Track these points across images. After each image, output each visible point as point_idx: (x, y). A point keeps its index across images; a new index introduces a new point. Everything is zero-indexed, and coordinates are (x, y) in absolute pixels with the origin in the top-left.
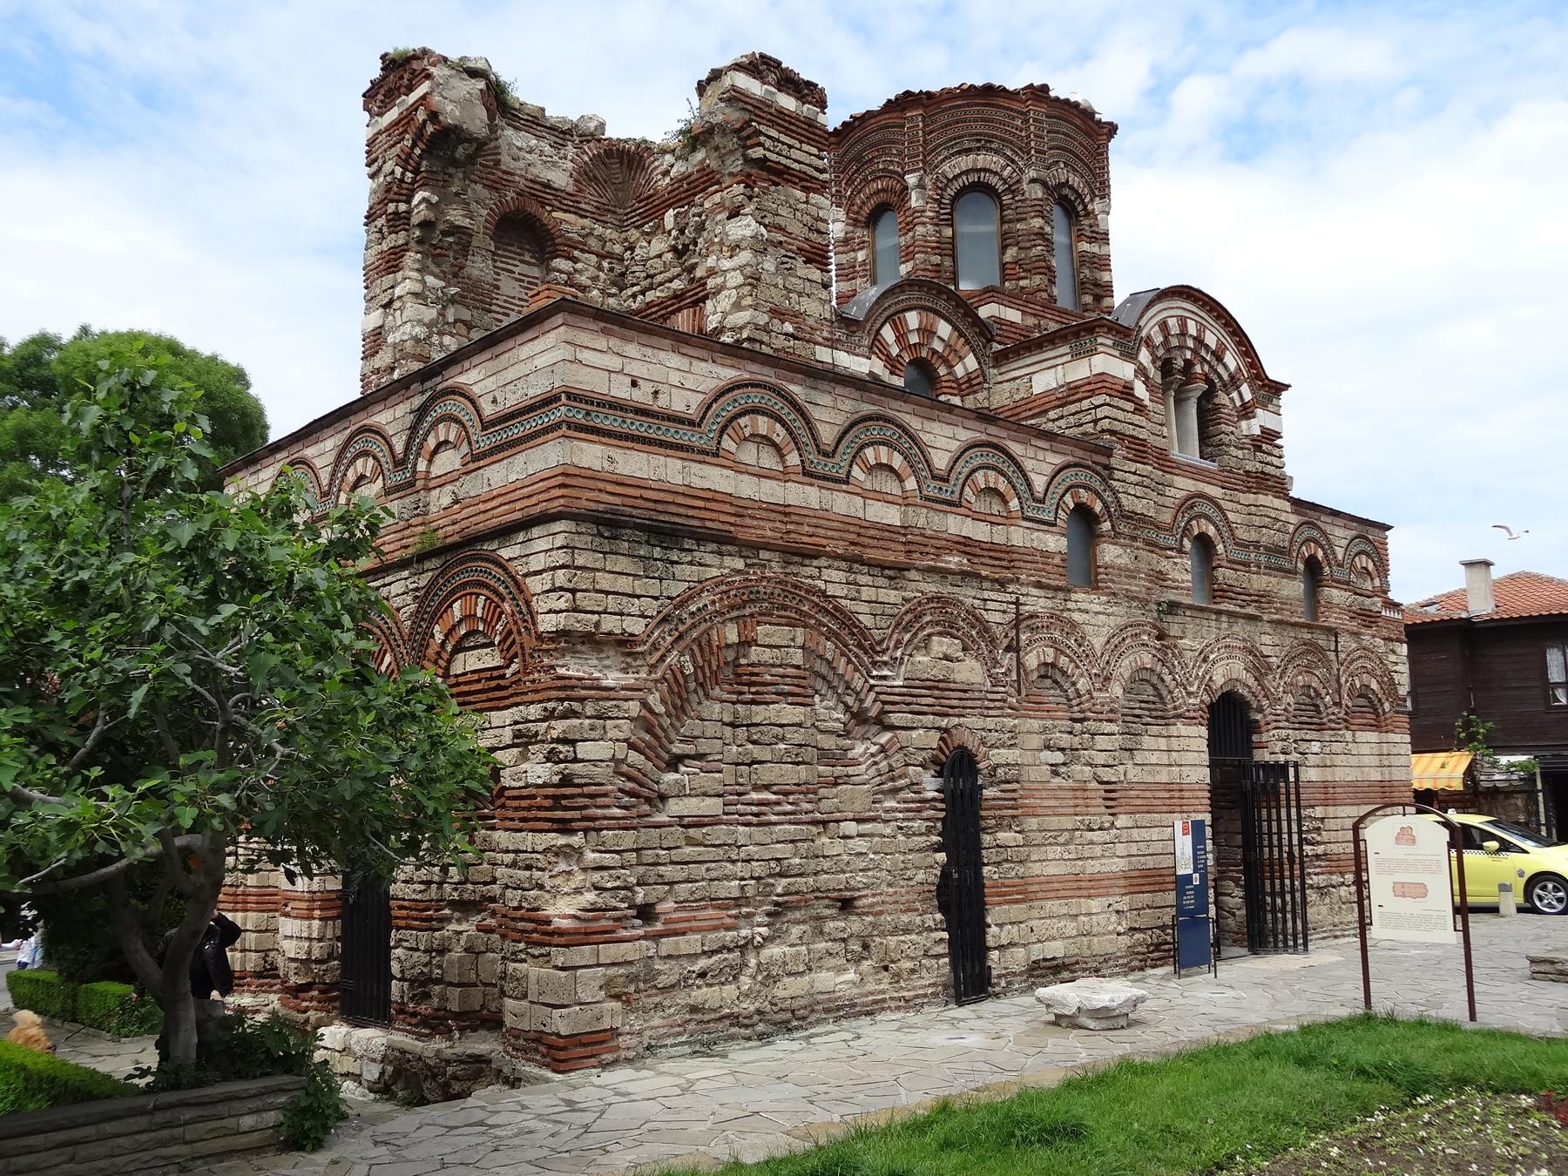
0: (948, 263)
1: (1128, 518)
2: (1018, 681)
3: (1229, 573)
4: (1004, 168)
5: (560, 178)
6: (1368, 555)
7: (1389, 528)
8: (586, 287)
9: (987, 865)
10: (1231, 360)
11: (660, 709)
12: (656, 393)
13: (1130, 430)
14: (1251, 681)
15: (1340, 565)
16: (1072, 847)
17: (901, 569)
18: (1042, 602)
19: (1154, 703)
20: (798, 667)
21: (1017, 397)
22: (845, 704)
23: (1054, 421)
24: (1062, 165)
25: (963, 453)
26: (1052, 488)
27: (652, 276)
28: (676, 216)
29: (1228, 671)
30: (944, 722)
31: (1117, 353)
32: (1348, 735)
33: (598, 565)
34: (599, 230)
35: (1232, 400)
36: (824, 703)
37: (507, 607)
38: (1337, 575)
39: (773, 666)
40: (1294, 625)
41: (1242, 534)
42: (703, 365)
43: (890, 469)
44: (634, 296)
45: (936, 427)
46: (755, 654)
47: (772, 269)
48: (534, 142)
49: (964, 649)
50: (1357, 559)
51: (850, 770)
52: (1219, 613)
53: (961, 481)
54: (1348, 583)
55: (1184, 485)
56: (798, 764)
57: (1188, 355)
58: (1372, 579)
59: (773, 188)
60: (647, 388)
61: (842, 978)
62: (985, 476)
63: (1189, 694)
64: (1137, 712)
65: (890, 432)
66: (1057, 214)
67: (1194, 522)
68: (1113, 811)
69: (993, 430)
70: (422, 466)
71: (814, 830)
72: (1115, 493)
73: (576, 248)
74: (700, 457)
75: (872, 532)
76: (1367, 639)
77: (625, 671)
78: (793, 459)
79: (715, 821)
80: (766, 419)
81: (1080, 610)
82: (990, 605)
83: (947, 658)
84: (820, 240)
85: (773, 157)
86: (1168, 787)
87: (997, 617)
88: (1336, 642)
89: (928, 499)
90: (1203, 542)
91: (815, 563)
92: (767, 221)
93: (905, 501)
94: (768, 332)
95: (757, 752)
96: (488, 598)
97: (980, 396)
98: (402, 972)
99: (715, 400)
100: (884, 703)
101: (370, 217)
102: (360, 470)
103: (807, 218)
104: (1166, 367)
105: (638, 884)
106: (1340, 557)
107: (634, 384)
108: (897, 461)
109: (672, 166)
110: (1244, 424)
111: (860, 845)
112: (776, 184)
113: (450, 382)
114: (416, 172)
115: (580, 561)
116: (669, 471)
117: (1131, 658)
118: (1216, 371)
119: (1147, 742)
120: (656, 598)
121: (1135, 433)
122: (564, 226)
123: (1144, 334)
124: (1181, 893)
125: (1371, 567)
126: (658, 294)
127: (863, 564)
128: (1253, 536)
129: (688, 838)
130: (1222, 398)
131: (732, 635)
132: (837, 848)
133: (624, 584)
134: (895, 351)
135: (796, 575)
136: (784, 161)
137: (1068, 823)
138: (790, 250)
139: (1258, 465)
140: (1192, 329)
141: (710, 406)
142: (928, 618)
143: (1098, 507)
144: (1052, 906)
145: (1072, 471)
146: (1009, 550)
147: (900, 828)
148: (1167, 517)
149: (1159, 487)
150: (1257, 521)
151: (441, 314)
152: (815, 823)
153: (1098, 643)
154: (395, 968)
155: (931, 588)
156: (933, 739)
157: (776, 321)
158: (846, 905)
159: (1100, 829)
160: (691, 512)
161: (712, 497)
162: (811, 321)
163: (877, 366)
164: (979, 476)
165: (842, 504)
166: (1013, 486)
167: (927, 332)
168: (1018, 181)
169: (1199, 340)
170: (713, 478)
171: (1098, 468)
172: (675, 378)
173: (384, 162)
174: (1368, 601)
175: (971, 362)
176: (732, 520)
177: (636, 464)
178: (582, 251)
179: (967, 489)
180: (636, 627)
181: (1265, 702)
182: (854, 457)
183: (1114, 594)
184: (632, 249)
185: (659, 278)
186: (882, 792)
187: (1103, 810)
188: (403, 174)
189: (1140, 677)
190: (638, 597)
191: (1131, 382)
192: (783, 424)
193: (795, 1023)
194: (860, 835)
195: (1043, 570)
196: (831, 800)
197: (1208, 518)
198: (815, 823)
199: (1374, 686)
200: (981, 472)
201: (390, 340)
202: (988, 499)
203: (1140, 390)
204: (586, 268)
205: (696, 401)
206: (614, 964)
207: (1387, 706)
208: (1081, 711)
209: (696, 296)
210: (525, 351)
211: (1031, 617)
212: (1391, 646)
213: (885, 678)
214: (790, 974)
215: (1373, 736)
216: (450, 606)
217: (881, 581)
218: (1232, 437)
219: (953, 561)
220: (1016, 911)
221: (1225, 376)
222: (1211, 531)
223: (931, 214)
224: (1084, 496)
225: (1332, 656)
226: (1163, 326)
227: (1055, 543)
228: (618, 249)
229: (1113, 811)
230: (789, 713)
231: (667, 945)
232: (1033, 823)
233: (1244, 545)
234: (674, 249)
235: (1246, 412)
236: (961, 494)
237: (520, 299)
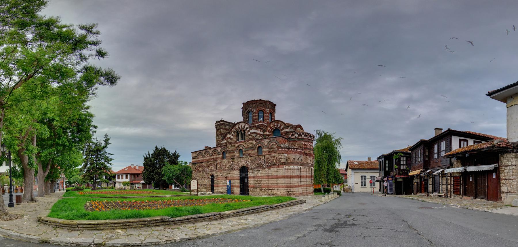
13: (230, 142)
17: (208, 162)
29: (242, 163)
32: (266, 169)
38: (264, 147)
40: (254, 156)
46: (200, 170)
55: (237, 144)
57: (240, 129)
76: (273, 155)
86: (234, 177)
95: (200, 176)
104: (237, 132)
111: (207, 182)
119: (231, 172)
124: (227, 187)
125: (275, 143)
137: (222, 180)
146: (217, 158)
148: (235, 149)
149: (234, 146)
161: (198, 161)
165: (205, 158)
169: (241, 127)
170: (198, 159)
181: (248, 167)
189: (230, 166)
199: (275, 161)
209: (26, 190)
212: (280, 155)
215: (275, 169)
219: (212, 160)
220: (217, 187)
225: (264, 159)
227: (221, 156)
233: (247, 148)
235: (249, 131)
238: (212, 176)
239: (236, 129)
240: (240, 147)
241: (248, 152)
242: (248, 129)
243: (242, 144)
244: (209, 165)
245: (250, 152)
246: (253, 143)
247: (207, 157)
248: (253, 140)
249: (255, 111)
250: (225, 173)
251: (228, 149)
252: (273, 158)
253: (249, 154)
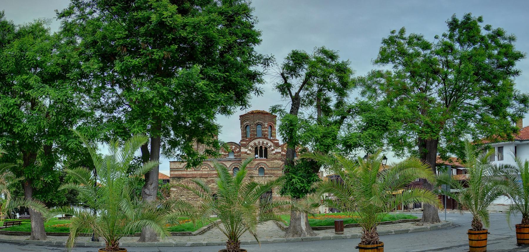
0: (245, 135)
10: (269, 145)
41: (270, 166)
55: (257, 162)
65: (205, 165)
78: (193, 169)
116: (180, 173)
130: (268, 149)
140: (261, 142)
148: (254, 166)
155: (211, 179)
161: (183, 174)
165: (199, 172)
169: (263, 143)
170: (185, 173)
177: (176, 173)
196: (198, 199)
219: (214, 176)
222: (263, 166)
224: (236, 166)
235: (273, 150)
239: (255, 144)
241: (273, 172)
242: (272, 148)
243: (263, 162)
244: (209, 181)
245: (276, 172)
246: (279, 163)
247: (205, 171)
248: (279, 160)
249: (266, 126)
253: (273, 174)
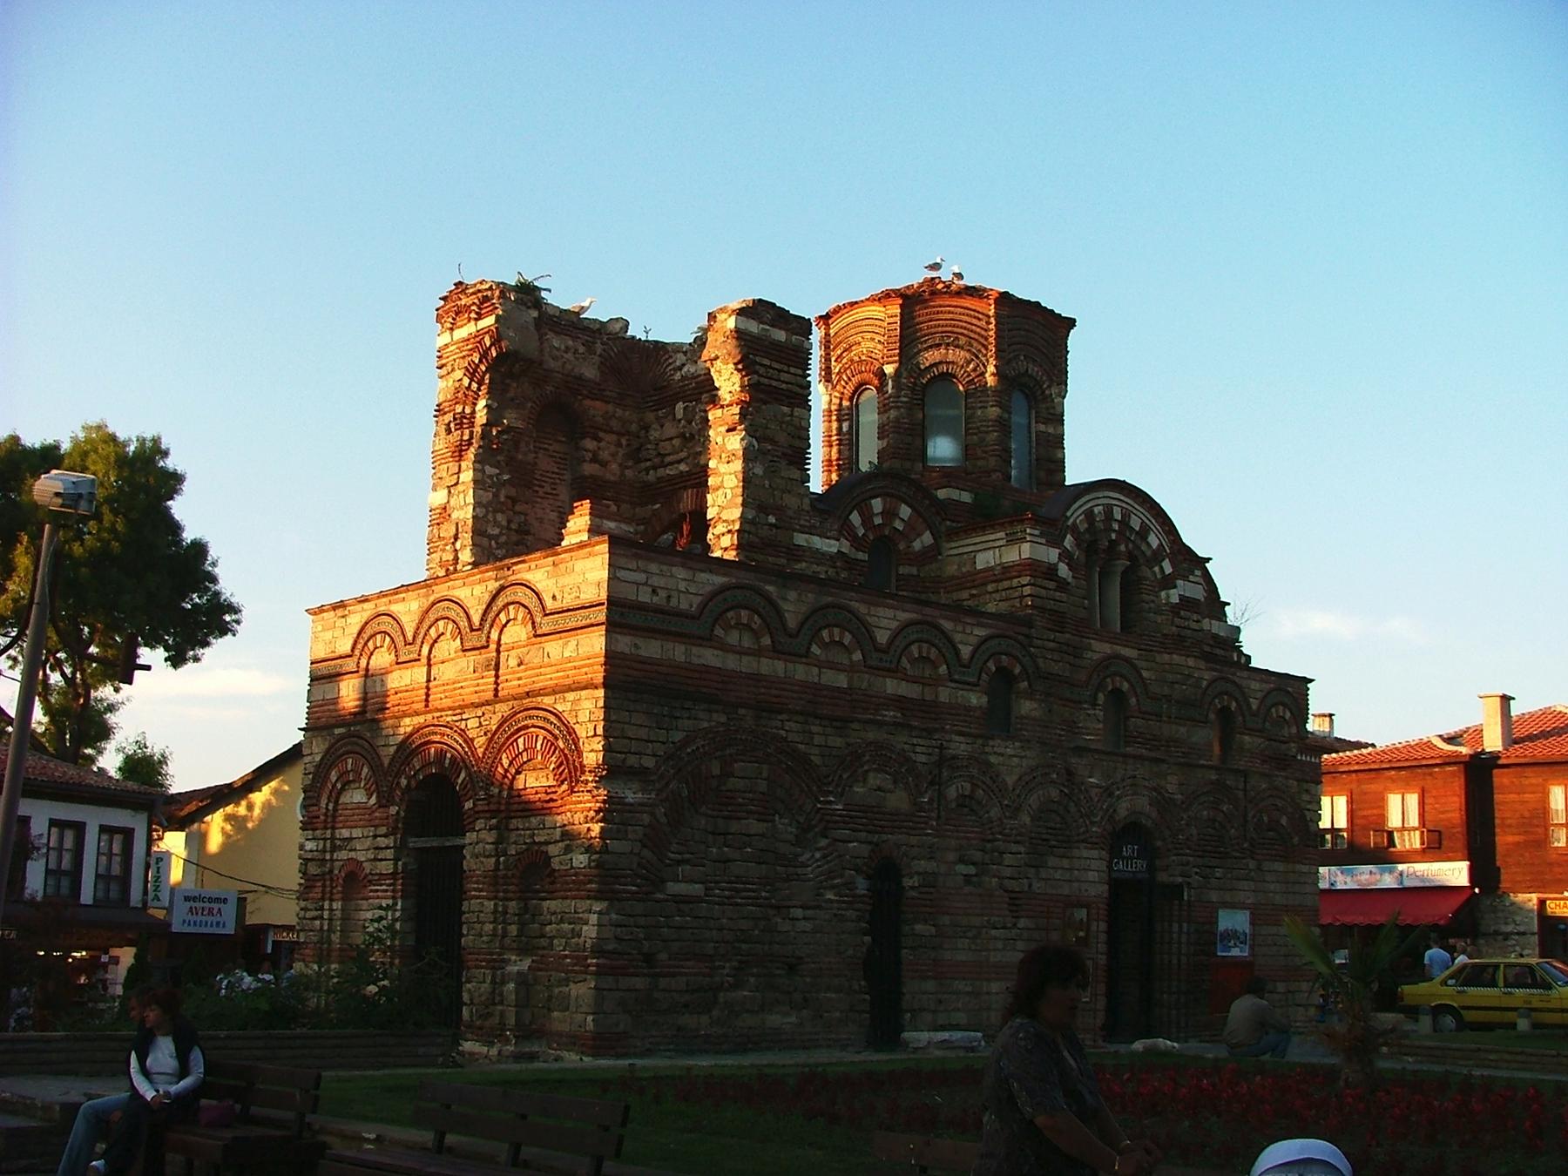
1: (1044, 678)
2: (938, 809)
3: (1140, 722)
4: (969, 363)
5: (590, 372)
6: (1285, 705)
7: (1311, 681)
8: (607, 462)
9: (905, 948)
10: (1154, 541)
11: (663, 820)
12: (669, 597)
13: (1051, 605)
14: (1154, 815)
15: (1254, 715)
16: (979, 941)
18: (963, 747)
19: (1060, 829)
20: (763, 794)
21: (964, 570)
22: (798, 822)
23: (991, 593)
24: (1022, 358)
25: (902, 630)
26: (977, 656)
27: (666, 455)
28: (685, 408)
30: (875, 838)
31: (1043, 541)
32: (1252, 864)
33: (627, 720)
34: (619, 412)
35: (1154, 573)
36: (783, 820)
37: (561, 744)
39: (745, 792)
40: (1203, 766)
42: (702, 575)
43: (840, 644)
44: (647, 470)
45: (881, 611)
46: (732, 783)
47: (761, 473)
48: (570, 343)
49: (895, 782)
50: (1273, 710)
51: (799, 871)
52: (1125, 756)
53: (898, 653)
54: (1260, 731)
55: (1101, 648)
56: (759, 863)
58: (1289, 727)
59: (764, 407)
60: (663, 594)
61: (785, 1021)
62: (920, 648)
63: (1092, 823)
64: (1044, 837)
66: (1019, 401)
67: (1109, 680)
68: (1015, 914)
69: (928, 611)
70: (494, 635)
71: (771, 912)
72: (1032, 656)
73: (601, 430)
74: (700, 641)
75: (825, 693)
77: (644, 791)
78: (767, 641)
79: (697, 900)
80: (747, 612)
81: (995, 753)
82: (918, 749)
83: (879, 789)
84: (801, 445)
85: (766, 381)
87: (923, 759)
88: (1245, 782)
89: (871, 667)
90: (1117, 696)
91: (779, 717)
92: (758, 435)
93: (851, 669)
94: (755, 524)
96: (545, 738)
97: (934, 566)
98: (471, 1000)
99: (711, 600)
100: (828, 822)
101: (440, 411)
102: (441, 630)
103: (791, 429)
105: (645, 939)
106: (1254, 707)
107: (654, 591)
108: (848, 638)
109: (684, 365)
110: (1163, 594)
111: (808, 926)
112: (765, 403)
113: (518, 576)
114: (480, 383)
115: (613, 718)
117: (1041, 792)
118: (1139, 548)
120: (664, 743)
121: (1055, 608)
122: (592, 412)
123: (1070, 522)
125: (1288, 715)
126: (668, 472)
127: (816, 717)
128: (1166, 691)
129: (679, 910)
131: (716, 771)
132: (785, 926)
133: (643, 733)
134: (861, 532)
135: (764, 726)
136: (774, 383)
138: (777, 456)
139: (1174, 628)
141: (707, 604)
142: (867, 758)
143: (1017, 670)
144: (960, 985)
145: (996, 641)
147: (835, 915)
150: (1170, 677)
151: (496, 495)
152: (772, 906)
153: (1010, 780)
154: (466, 997)
155: (871, 735)
156: (865, 850)
157: (762, 515)
158: (792, 968)
159: (1003, 928)
160: (690, 682)
161: (707, 669)
162: (790, 513)
163: (845, 545)
164: (914, 649)
165: (800, 672)
166: (944, 656)
167: (890, 514)
168: (983, 374)
169: (1124, 523)
170: (709, 657)
171: (1020, 637)
172: (682, 586)
173: (453, 370)
174: (1284, 747)
175: (927, 538)
176: (720, 686)
177: (652, 649)
178: (605, 431)
179: (904, 660)
180: (649, 762)
182: (813, 637)
183: (1029, 741)
184: (647, 428)
185: (668, 459)
186: (825, 888)
187: (1007, 913)
188: (470, 384)
190: (652, 742)
191: (1056, 565)
192: (760, 615)
193: (750, 1046)
194: (804, 918)
195: (966, 721)
197: (1122, 676)
198: (772, 906)
199: (1284, 821)
200: (917, 645)
201: (455, 515)
202: (921, 666)
203: (1064, 570)
204: (607, 447)
205: (696, 600)
206: (628, 990)
207: (1296, 840)
208: (992, 834)
210: (580, 565)
211: (954, 757)
212: (1305, 786)
213: (830, 802)
214: (747, 1011)
215: (1279, 866)
216: (516, 740)
217: (829, 730)
218: (1152, 605)
219: (890, 714)
220: (930, 985)
221: (1149, 553)
222: (1126, 686)
223: (905, 399)
225: (1241, 794)
226: (1089, 514)
228: (634, 427)
229: (1015, 914)
230: (755, 826)
231: (663, 982)
232: (946, 920)
234: (682, 436)
235: (1168, 582)
236: (899, 662)
237: (553, 473)
238: (885, 872)
240: (1115, 674)
250: (1008, 860)
251: (1040, 661)
252: (1280, 803)
